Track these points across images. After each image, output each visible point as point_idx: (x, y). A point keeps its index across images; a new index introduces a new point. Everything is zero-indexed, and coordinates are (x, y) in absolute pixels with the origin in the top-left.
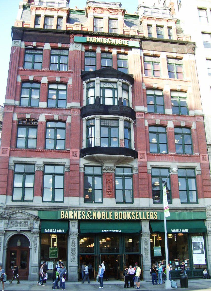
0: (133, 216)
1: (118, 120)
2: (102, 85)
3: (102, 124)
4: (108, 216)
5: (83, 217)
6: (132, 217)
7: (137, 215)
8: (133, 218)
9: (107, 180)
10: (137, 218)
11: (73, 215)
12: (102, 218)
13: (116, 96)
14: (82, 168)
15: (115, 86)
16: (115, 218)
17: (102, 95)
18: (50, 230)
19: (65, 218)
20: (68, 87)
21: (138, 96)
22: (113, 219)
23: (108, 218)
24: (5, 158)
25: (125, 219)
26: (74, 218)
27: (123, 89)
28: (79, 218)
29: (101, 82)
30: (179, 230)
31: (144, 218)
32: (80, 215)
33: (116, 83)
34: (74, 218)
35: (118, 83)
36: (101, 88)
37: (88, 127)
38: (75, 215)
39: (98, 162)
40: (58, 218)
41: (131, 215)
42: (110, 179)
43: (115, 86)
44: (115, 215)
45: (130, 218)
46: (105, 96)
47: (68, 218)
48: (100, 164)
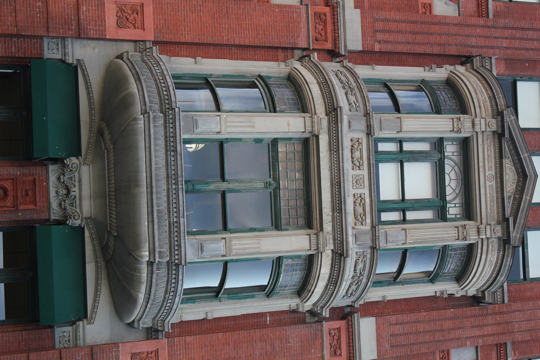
1: (309, 225)
2: (450, 149)
3: (281, 148)
9: (8, 185)
13: (411, 215)
14: (65, 54)
15: (453, 210)
17: (407, 147)
21: (421, 327)
27: (443, 253)
29: (465, 145)
33: (469, 211)
35: (471, 223)
36: (439, 144)
39: (100, 132)
42: (15, 198)
43: (453, 210)
46: (406, 165)
48: (89, 143)
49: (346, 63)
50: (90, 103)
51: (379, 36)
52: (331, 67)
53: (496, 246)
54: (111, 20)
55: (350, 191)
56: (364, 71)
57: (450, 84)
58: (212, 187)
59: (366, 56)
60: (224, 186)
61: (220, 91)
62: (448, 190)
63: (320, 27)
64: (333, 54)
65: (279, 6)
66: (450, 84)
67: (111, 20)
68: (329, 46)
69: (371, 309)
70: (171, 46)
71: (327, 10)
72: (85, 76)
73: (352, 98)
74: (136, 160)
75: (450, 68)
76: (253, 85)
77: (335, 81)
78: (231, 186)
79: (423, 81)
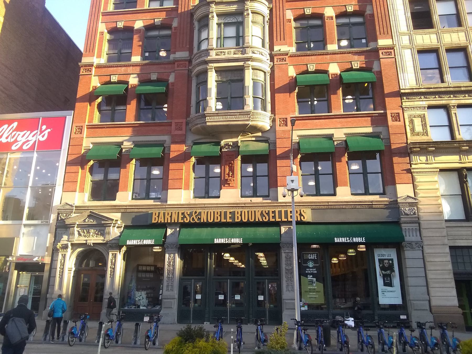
0: (264, 216)
4: (225, 218)
5: (185, 219)
6: (264, 218)
7: (271, 215)
8: (266, 219)
10: (272, 220)
11: (171, 217)
12: (216, 221)
13: (241, 35)
16: (236, 220)
18: (135, 241)
19: (159, 222)
20: (173, 31)
22: (233, 222)
23: (225, 221)
24: (78, 139)
25: (246, 221)
26: (173, 221)
28: (180, 221)
30: (348, 238)
31: (284, 219)
32: (182, 216)
34: (173, 221)
37: (198, 84)
38: (175, 217)
39: (213, 136)
40: (149, 223)
41: (262, 214)
43: (240, 19)
44: (236, 215)
45: (261, 220)
47: (163, 222)
49: (192, 57)
50: (205, 139)
51: (184, 45)
52: (194, 62)
53: (252, 3)
54: (179, 132)
55: (232, 56)
56: (195, 51)
57: (199, 21)
58: (229, 101)
59: (191, 50)
60: (229, 98)
61: (201, 99)
62: (233, 21)
63: (182, 66)
64: (190, 61)
65: (175, 79)
66: (199, 21)
67: (179, 132)
68: (187, 63)
69: (271, 48)
70: (188, 113)
71: (176, 63)
72: (197, 140)
73: (203, 55)
74: (220, 125)
75: (194, 21)
76: (199, 88)
77: (198, 61)
78: (229, 95)
79: (199, 30)
